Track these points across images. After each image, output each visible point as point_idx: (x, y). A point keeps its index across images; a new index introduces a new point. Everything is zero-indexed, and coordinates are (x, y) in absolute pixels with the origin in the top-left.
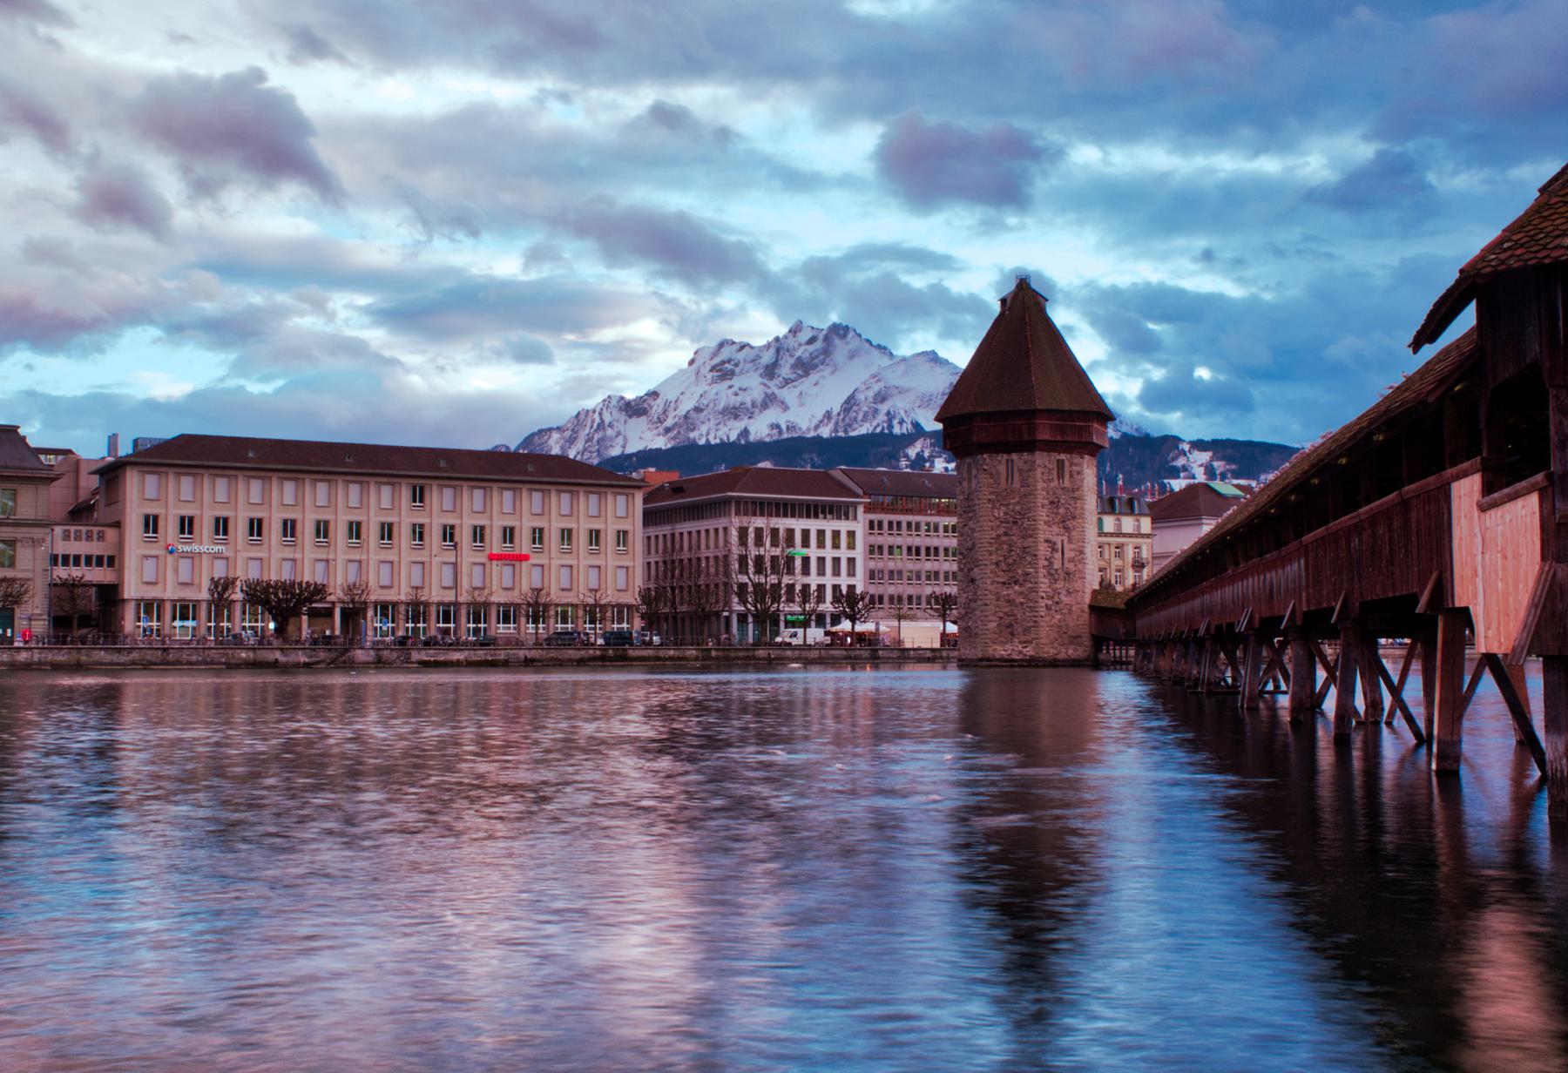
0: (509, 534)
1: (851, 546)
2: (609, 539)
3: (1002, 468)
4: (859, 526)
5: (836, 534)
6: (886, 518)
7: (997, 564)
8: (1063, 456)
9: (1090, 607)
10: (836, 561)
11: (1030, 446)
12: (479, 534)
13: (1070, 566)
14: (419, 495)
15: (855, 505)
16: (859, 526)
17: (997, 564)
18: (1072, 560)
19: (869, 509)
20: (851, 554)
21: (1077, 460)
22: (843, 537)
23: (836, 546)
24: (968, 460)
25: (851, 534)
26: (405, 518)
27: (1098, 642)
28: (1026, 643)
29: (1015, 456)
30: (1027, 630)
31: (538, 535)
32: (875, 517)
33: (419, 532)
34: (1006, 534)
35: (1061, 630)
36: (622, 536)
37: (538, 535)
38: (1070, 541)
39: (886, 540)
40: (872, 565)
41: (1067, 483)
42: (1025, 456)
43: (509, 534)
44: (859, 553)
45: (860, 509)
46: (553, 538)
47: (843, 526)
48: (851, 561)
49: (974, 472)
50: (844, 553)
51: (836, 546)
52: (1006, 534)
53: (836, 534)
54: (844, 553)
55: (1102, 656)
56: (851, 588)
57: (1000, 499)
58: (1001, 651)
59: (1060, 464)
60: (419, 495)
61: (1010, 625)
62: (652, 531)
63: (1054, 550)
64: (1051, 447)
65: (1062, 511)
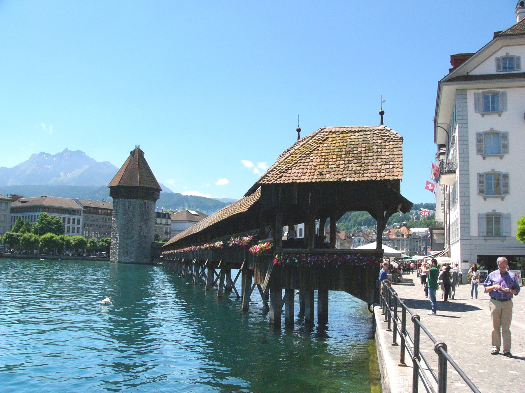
1: (78, 223)
3: (127, 203)
5: (74, 220)
7: (124, 233)
8: (146, 201)
9: (152, 247)
10: (74, 228)
11: (136, 198)
13: (146, 234)
17: (124, 233)
18: (146, 233)
19: (85, 212)
20: (78, 226)
21: (150, 202)
23: (74, 223)
24: (117, 200)
25: (79, 220)
28: (132, 257)
29: (131, 200)
32: (86, 214)
34: (127, 223)
38: (147, 227)
41: (147, 209)
42: (135, 200)
44: (81, 226)
45: (82, 212)
47: (76, 217)
48: (78, 228)
49: (119, 204)
50: (76, 226)
51: (74, 223)
52: (127, 223)
53: (74, 220)
54: (76, 226)
55: (154, 262)
58: (123, 260)
59: (145, 203)
61: (127, 252)
62: (13, 215)
63: (141, 229)
64: (142, 198)
65: (145, 217)
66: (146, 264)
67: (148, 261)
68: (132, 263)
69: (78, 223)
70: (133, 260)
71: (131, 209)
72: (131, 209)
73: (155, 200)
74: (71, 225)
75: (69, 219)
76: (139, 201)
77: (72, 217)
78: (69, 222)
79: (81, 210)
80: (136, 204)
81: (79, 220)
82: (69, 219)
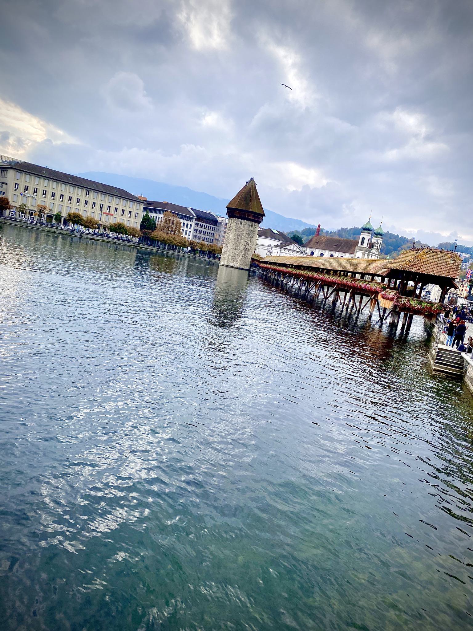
0: (109, 208)
1: (190, 228)
2: (133, 215)
3: (239, 223)
4: (193, 223)
5: (187, 224)
6: (200, 223)
11: (247, 219)
12: (102, 206)
14: (88, 193)
15: (193, 218)
16: (193, 223)
21: (256, 224)
22: (189, 226)
25: (191, 225)
26: (83, 198)
27: (251, 266)
28: (236, 263)
30: (237, 261)
31: (116, 210)
33: (86, 202)
35: (245, 262)
36: (137, 214)
37: (116, 210)
39: (199, 229)
40: (194, 234)
43: (109, 208)
44: (192, 230)
46: (120, 211)
47: (189, 223)
53: (187, 224)
54: (188, 230)
56: (189, 238)
57: (237, 230)
60: (88, 193)
64: (250, 220)
66: (246, 270)
67: (248, 268)
68: (236, 268)
69: (190, 228)
70: (237, 266)
71: (242, 227)
72: (242, 227)
73: (259, 222)
74: (185, 229)
75: (184, 223)
76: (248, 222)
77: (186, 222)
78: (184, 227)
79: (193, 218)
80: (246, 224)
81: (191, 225)
82: (184, 223)
